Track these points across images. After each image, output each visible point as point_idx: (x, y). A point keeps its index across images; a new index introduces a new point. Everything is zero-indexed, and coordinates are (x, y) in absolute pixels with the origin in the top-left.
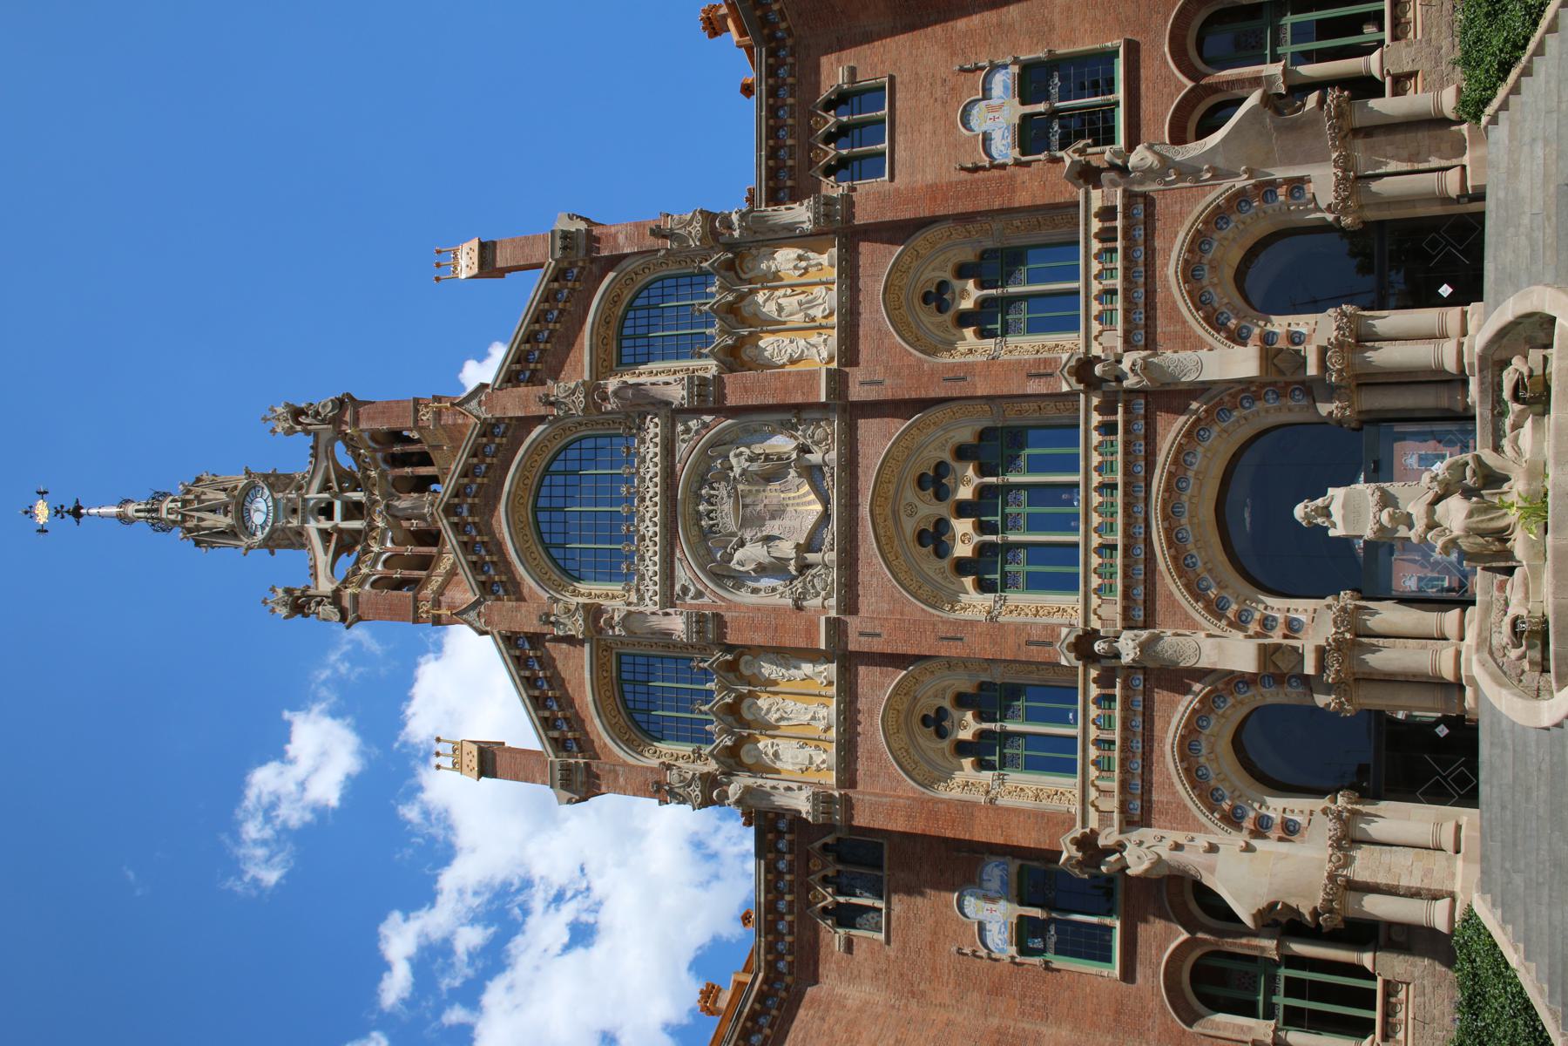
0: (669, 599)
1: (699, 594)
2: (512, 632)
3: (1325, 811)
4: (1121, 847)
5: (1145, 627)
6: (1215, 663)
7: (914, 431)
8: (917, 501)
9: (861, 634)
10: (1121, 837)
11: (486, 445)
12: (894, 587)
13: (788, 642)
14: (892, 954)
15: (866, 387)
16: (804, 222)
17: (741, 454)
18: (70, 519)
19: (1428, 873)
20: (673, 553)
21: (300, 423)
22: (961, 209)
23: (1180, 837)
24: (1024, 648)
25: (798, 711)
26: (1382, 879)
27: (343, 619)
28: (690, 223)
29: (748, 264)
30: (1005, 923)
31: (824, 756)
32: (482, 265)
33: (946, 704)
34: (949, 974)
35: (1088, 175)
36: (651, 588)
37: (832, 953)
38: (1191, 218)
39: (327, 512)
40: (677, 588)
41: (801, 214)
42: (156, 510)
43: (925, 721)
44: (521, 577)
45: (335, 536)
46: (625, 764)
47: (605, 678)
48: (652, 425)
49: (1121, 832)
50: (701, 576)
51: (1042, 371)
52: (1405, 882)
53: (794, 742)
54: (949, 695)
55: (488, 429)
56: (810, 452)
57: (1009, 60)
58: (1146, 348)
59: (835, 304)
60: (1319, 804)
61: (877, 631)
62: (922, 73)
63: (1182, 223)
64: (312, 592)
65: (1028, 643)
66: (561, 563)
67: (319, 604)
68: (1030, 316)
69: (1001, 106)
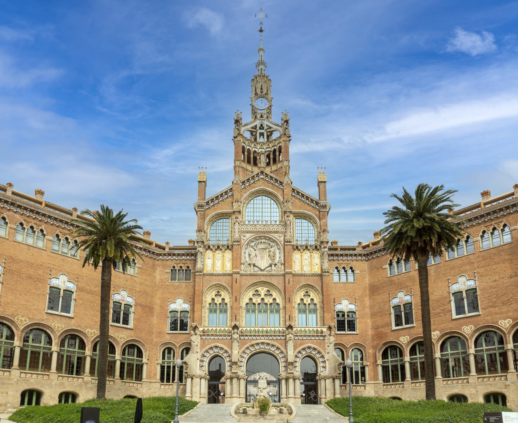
1: (244, 240)
3: (206, 374)
4: (196, 334)
5: (240, 339)
9: (236, 279)
11: (277, 182)
18: (259, 29)
19: (196, 392)
20: (252, 233)
21: (284, 123)
22: (324, 301)
23: (199, 346)
25: (219, 264)
26: (194, 385)
27: (235, 137)
29: (316, 251)
32: (320, 182)
35: (330, 328)
36: (245, 228)
38: (319, 348)
40: (245, 235)
41: (326, 265)
42: (262, 64)
43: (218, 292)
46: (204, 221)
58: (294, 339)
59: (306, 273)
60: (207, 372)
64: (241, 126)
66: (250, 203)
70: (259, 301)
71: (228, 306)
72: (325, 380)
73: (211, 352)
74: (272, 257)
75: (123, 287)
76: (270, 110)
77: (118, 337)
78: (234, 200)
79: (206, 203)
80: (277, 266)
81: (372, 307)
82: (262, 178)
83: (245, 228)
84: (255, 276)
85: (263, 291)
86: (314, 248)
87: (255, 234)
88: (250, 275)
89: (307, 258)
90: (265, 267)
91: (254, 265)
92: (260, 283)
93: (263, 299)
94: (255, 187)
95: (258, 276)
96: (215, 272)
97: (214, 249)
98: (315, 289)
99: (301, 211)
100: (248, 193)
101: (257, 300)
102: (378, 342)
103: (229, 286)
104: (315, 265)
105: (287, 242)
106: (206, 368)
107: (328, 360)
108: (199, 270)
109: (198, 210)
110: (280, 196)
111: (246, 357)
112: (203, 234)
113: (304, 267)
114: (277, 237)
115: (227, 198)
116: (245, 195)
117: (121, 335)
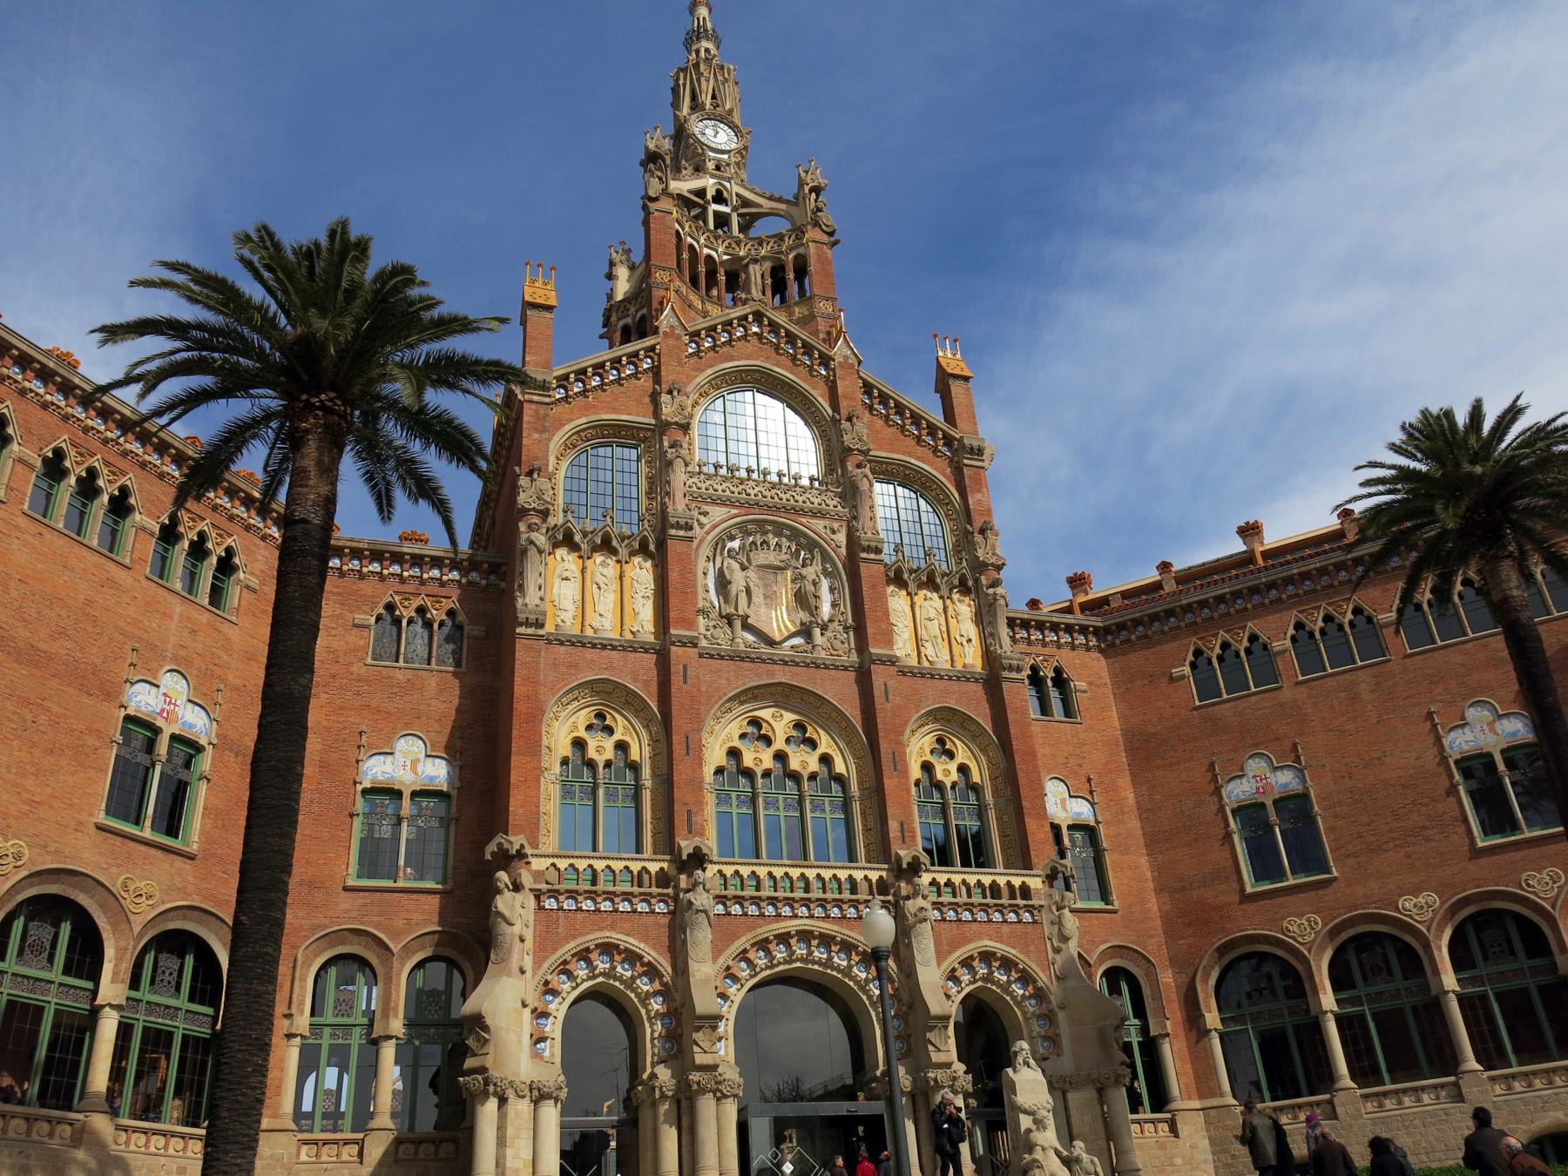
0: (697, 498)
1: (701, 525)
2: (659, 355)
6: (694, 976)
7: (844, 724)
8: (785, 721)
9: (685, 667)
10: (527, 889)
12: (720, 698)
13: (674, 602)
14: (355, 669)
15: (883, 687)
16: (1001, 648)
17: (817, 576)
20: (734, 506)
22: (1020, 774)
24: (685, 809)
25: (606, 603)
26: (510, 1131)
28: (994, 554)
30: (392, 777)
31: (568, 624)
33: (618, 736)
34: (338, 722)
36: (703, 486)
37: (352, 612)
38: (1025, 959)
39: (719, 198)
44: (703, 370)
45: (701, 202)
47: (619, 432)
48: (836, 503)
49: (531, 890)
50: (717, 530)
51: (906, 834)
52: (509, 1152)
53: (578, 597)
54: (627, 738)
55: (825, 360)
56: (822, 634)
57: (1100, 819)
59: (939, 666)
61: (689, 681)
62: (1084, 749)
63: (1021, 952)
65: (689, 812)
67: (660, 179)
68: (734, 815)
69: (1064, 808)
70: (768, 761)
71: (646, 772)
72: (1064, 1093)
73: (601, 966)
74: (803, 600)
75: (175, 659)
76: (743, 157)
77: (125, 887)
78: (665, 387)
79: (558, 379)
80: (829, 634)
81: (1146, 811)
82: (755, 334)
83: (703, 486)
84: (752, 660)
85: (781, 723)
86: (956, 582)
87: (743, 511)
88: (732, 659)
89: (932, 614)
90: (786, 634)
91: (747, 627)
92: (772, 690)
93: (780, 757)
94: (732, 359)
95: (764, 661)
96: (589, 632)
97: (584, 546)
98: (973, 728)
99: (896, 456)
100: (710, 371)
101: (758, 758)
102: (1190, 940)
103: (649, 694)
104: (965, 643)
105: (868, 549)
106: (553, 1050)
107: (1062, 1007)
108: (532, 617)
109: (527, 397)
110: (820, 399)
111: (737, 994)
112: (542, 482)
113: (928, 645)
114: (822, 531)
115: (635, 376)
116: (702, 378)
117: (143, 878)
